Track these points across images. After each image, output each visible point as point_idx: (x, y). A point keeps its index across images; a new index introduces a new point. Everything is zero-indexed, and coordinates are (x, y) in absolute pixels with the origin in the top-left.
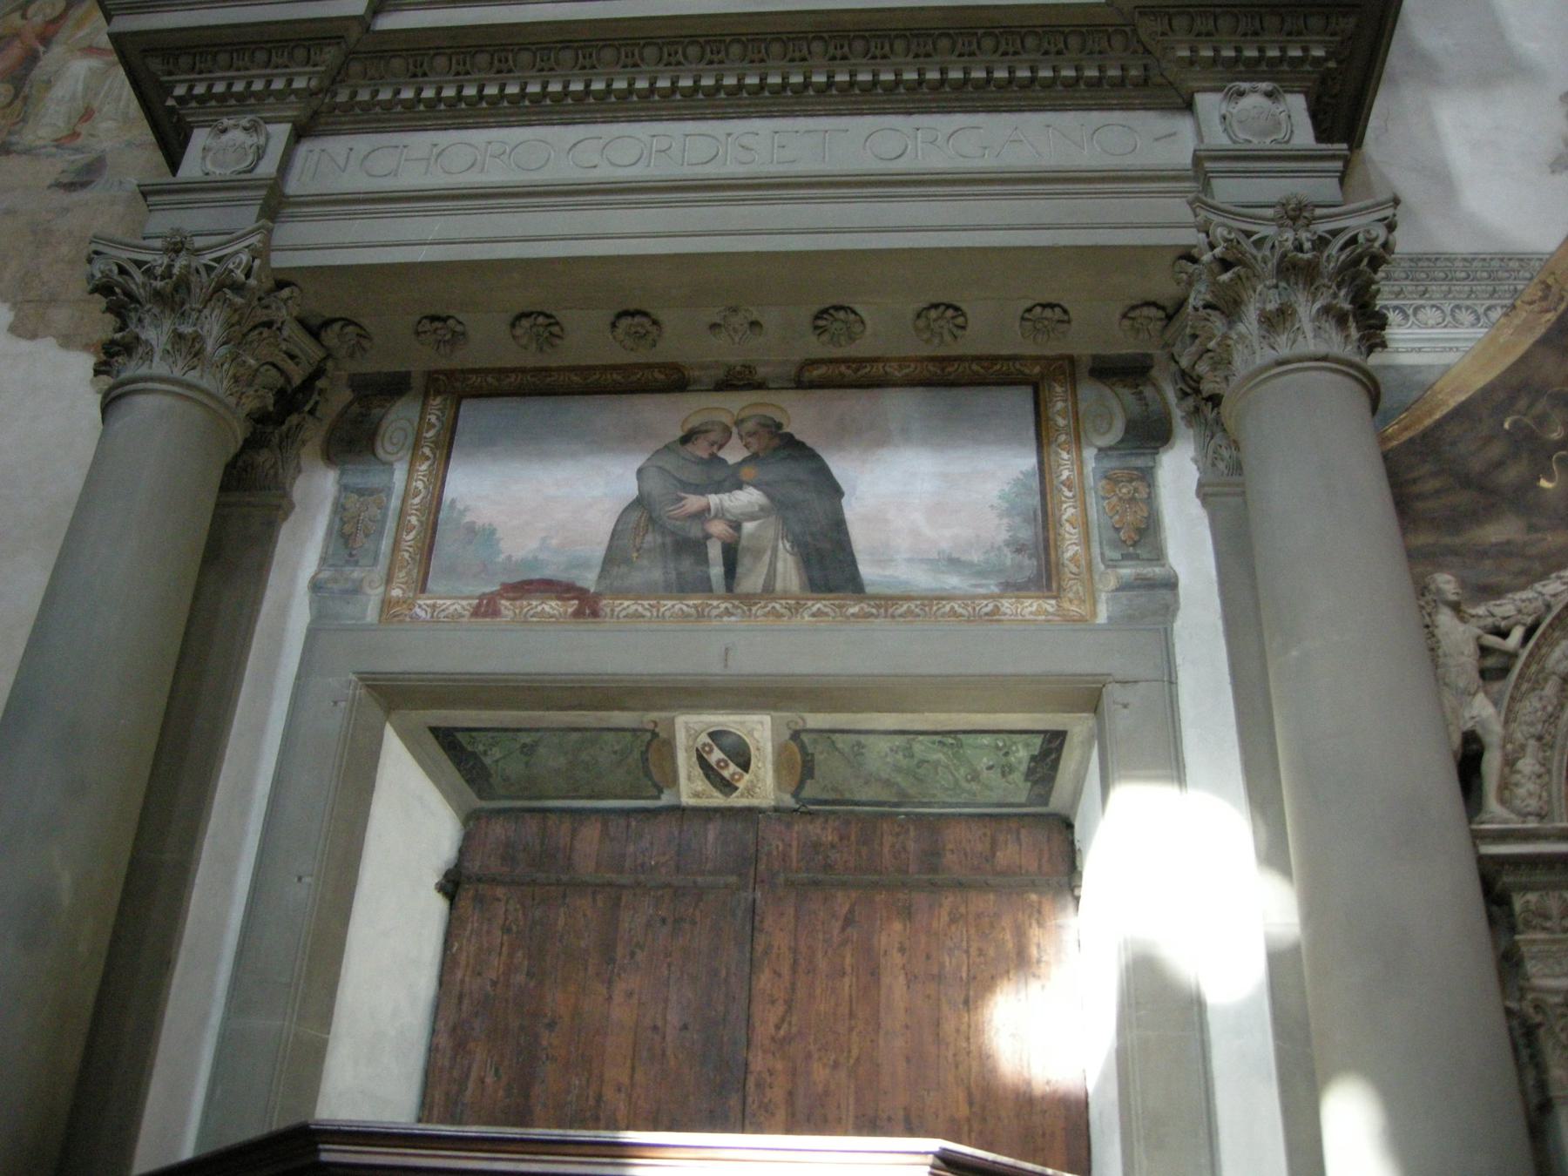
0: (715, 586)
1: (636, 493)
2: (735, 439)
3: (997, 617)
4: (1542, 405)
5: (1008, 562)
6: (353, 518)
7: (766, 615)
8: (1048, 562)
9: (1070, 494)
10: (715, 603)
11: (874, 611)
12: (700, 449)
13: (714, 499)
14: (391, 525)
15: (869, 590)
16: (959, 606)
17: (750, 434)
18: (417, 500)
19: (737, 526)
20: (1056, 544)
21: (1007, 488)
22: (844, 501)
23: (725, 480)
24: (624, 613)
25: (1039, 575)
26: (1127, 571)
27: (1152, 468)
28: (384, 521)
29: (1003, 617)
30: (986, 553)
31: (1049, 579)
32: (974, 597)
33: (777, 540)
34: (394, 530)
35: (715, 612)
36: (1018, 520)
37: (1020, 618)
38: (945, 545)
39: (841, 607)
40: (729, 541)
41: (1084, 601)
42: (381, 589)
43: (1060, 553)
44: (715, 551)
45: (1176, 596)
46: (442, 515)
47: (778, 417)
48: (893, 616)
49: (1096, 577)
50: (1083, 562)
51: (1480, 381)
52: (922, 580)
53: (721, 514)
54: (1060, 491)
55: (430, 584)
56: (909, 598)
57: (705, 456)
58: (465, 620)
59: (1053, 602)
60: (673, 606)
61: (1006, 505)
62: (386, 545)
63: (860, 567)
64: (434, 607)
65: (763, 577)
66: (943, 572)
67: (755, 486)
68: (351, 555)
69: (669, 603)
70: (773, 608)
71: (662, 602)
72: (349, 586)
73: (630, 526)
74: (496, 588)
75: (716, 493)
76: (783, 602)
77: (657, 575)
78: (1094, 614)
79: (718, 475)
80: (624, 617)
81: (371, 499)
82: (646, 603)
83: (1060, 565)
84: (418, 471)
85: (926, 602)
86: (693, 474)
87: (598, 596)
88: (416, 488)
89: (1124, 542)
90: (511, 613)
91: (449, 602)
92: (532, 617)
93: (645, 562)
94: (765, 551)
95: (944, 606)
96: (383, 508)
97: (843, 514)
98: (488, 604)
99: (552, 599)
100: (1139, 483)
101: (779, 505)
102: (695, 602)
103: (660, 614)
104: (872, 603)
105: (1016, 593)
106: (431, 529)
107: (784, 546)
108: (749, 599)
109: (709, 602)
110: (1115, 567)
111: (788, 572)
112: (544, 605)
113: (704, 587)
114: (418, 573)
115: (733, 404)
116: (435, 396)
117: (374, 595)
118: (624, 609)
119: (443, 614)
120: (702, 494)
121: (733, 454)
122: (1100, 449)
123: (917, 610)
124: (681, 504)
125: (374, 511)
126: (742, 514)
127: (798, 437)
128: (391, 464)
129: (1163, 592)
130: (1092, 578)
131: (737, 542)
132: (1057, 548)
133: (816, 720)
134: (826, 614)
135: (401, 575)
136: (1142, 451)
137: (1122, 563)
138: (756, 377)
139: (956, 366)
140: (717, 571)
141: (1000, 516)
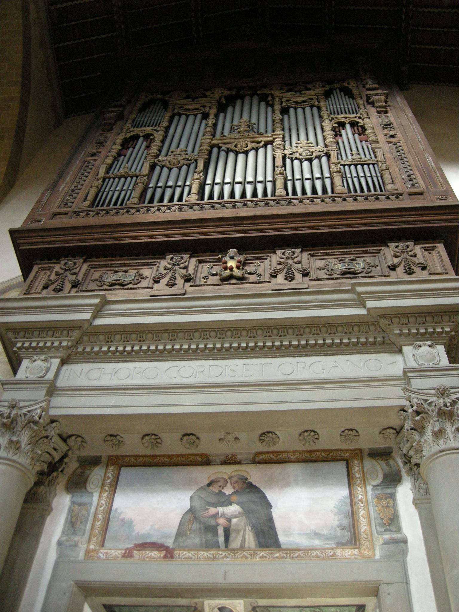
0: (220, 546)
2: (229, 484)
3: (335, 557)
5: (339, 534)
6: (76, 515)
7: (241, 558)
8: (355, 533)
9: (362, 505)
10: (221, 552)
11: (285, 555)
12: (215, 489)
13: (220, 509)
14: (91, 518)
15: (283, 547)
16: (320, 553)
17: (235, 483)
18: (102, 508)
19: (229, 520)
20: (358, 526)
21: (337, 503)
22: (272, 510)
23: (225, 501)
24: (184, 557)
25: (351, 539)
26: (387, 536)
27: (394, 493)
28: (88, 517)
29: (337, 557)
30: (329, 530)
31: (355, 541)
33: (246, 526)
34: (92, 520)
35: (221, 556)
36: (342, 516)
37: (344, 557)
38: (313, 527)
39: (271, 554)
40: (226, 526)
41: (370, 549)
42: (85, 546)
43: (359, 529)
44: (221, 531)
45: (407, 546)
46: (112, 515)
47: (246, 475)
48: (293, 558)
49: (374, 539)
50: (369, 533)
52: (304, 542)
53: (223, 515)
54: (358, 504)
55: (106, 543)
56: (299, 550)
57: (217, 491)
58: (119, 559)
59: (357, 550)
60: (204, 554)
61: (337, 510)
62: (89, 526)
63: (279, 537)
64: (107, 553)
65: (240, 542)
66: (313, 539)
67: (237, 504)
68: (74, 531)
69: (202, 553)
70: (244, 555)
71: (200, 552)
72: (73, 543)
73: (187, 520)
75: (221, 507)
76: (248, 552)
77: (197, 541)
78: (374, 555)
79: (223, 499)
80: (185, 558)
81: (83, 508)
82: (192, 553)
83: (359, 534)
84: (103, 496)
85: (306, 551)
86: (212, 499)
87: (174, 549)
88: (102, 503)
89: (385, 524)
90: (138, 556)
91: (113, 551)
92: (147, 558)
93: (193, 536)
94: (241, 531)
95: (313, 553)
96: (88, 511)
97: (272, 515)
98: (129, 553)
99: (153, 550)
100: (390, 499)
101: (247, 512)
102: (213, 552)
103: (198, 557)
104: (284, 552)
105: (343, 547)
107: (248, 529)
108: (234, 551)
109: (219, 552)
110: (382, 535)
111: (250, 539)
112: (151, 553)
113: (216, 546)
114: (101, 538)
115: (229, 470)
116: (111, 466)
118: (184, 555)
119: (110, 557)
120: (216, 507)
121: (228, 491)
122: (373, 486)
123: (302, 555)
124: (207, 511)
125: (85, 512)
126: (232, 515)
127: (254, 483)
128: (92, 493)
129: (402, 545)
130: (372, 539)
131: (230, 527)
132: (358, 527)
133: (263, 602)
134: (266, 557)
135: (94, 539)
136: (390, 486)
137: (385, 533)
138: (237, 459)
139: (316, 454)
140: (221, 539)
141: (335, 515)
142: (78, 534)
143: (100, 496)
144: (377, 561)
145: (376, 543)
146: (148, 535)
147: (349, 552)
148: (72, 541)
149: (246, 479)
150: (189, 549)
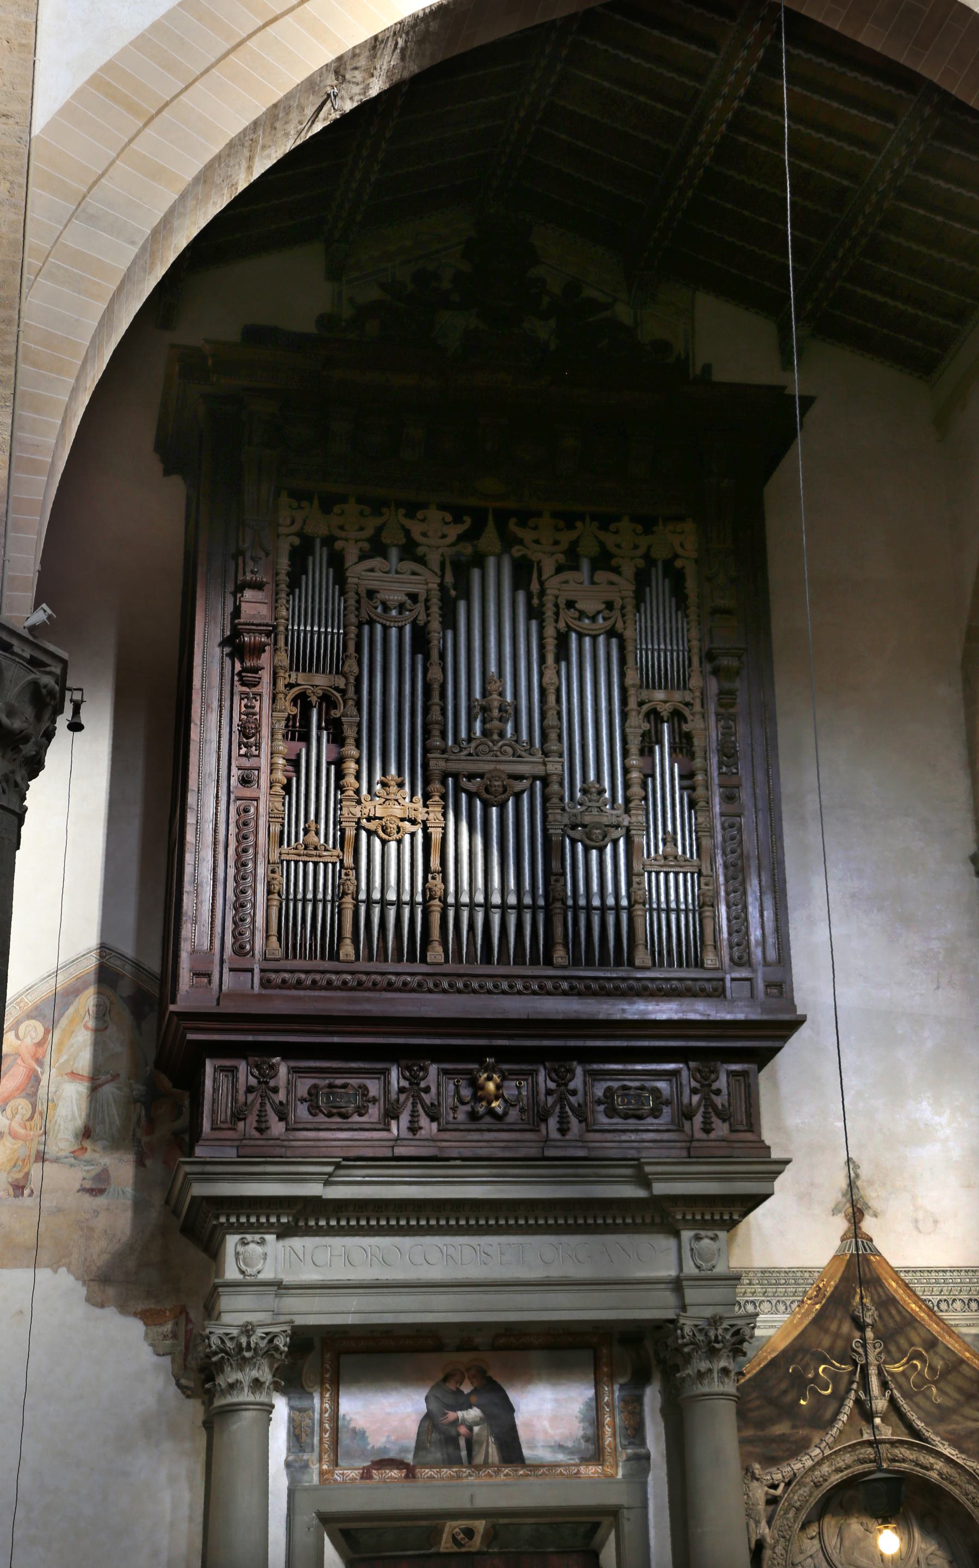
1: (426, 1411)
4: (807, 1358)
5: (583, 1447)
7: (486, 1476)
8: (599, 1446)
9: (608, 1410)
12: (451, 1386)
13: (460, 1414)
14: (317, 1428)
15: (527, 1462)
18: (327, 1415)
19: (470, 1429)
22: (515, 1414)
32: (569, 1465)
35: (464, 1475)
36: (587, 1424)
38: (557, 1438)
39: (516, 1471)
42: (317, 1465)
44: (462, 1443)
46: (340, 1423)
49: (618, 1454)
51: (782, 1346)
52: (547, 1456)
53: (464, 1421)
54: (604, 1408)
56: (543, 1466)
57: (454, 1389)
59: (600, 1467)
62: (316, 1440)
64: (343, 1474)
66: (557, 1453)
67: (478, 1407)
68: (301, 1446)
69: (445, 1470)
72: (303, 1464)
74: (369, 1464)
78: (617, 1473)
80: (428, 1477)
81: (305, 1415)
83: (604, 1448)
87: (414, 1467)
91: (349, 1472)
93: (433, 1449)
96: (312, 1419)
101: (488, 1418)
106: (336, 1430)
107: (491, 1440)
108: (478, 1468)
110: (625, 1449)
111: (493, 1453)
115: (465, 1358)
117: (315, 1467)
119: (348, 1478)
121: (466, 1388)
126: (473, 1422)
128: (311, 1394)
134: (510, 1475)
135: (325, 1457)
140: (464, 1453)
141: (580, 1422)
142: (306, 1450)
143: (322, 1397)
144: (619, 1482)
145: (619, 1459)
146: (384, 1450)
147: (591, 1471)
148: (301, 1460)
149: (485, 1372)
150: (431, 1466)
